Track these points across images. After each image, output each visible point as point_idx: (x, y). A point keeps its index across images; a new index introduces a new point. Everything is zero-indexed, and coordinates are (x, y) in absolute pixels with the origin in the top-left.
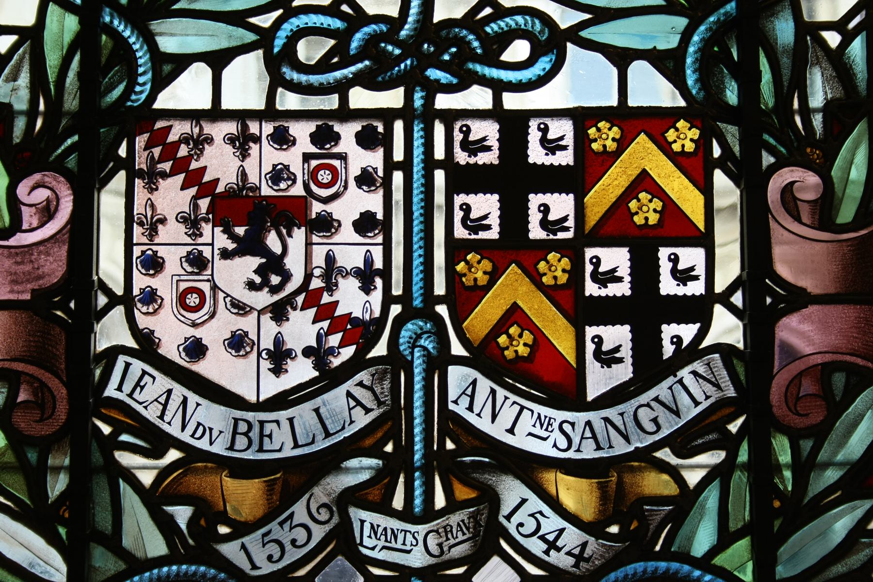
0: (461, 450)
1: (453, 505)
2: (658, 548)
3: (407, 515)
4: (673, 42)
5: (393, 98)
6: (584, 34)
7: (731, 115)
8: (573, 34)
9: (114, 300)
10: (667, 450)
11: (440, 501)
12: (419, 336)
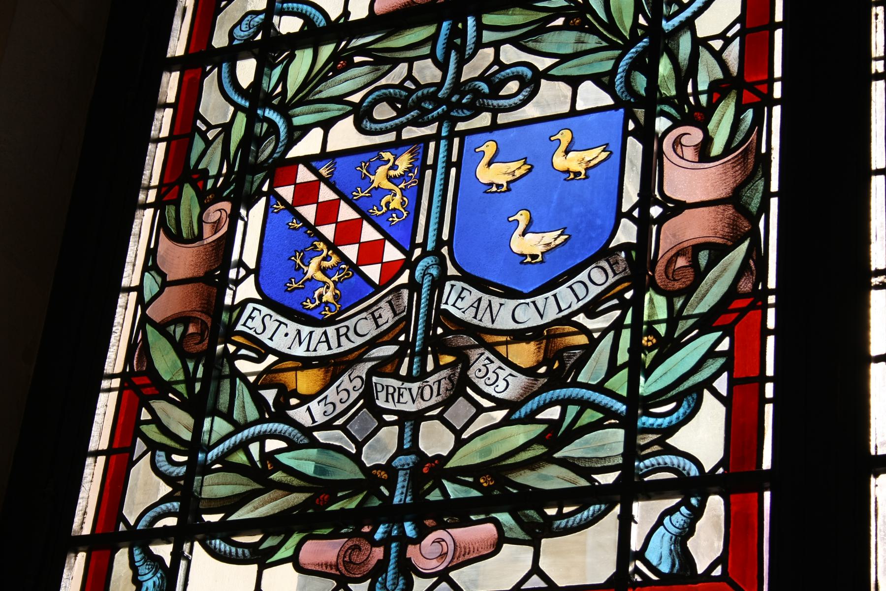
0: (447, 331)
1: (438, 368)
2: (569, 381)
3: (409, 378)
4: (608, 66)
6: (553, 72)
7: (640, 102)
8: (546, 75)
9: (249, 272)
10: (582, 315)
11: (430, 367)
12: (428, 268)
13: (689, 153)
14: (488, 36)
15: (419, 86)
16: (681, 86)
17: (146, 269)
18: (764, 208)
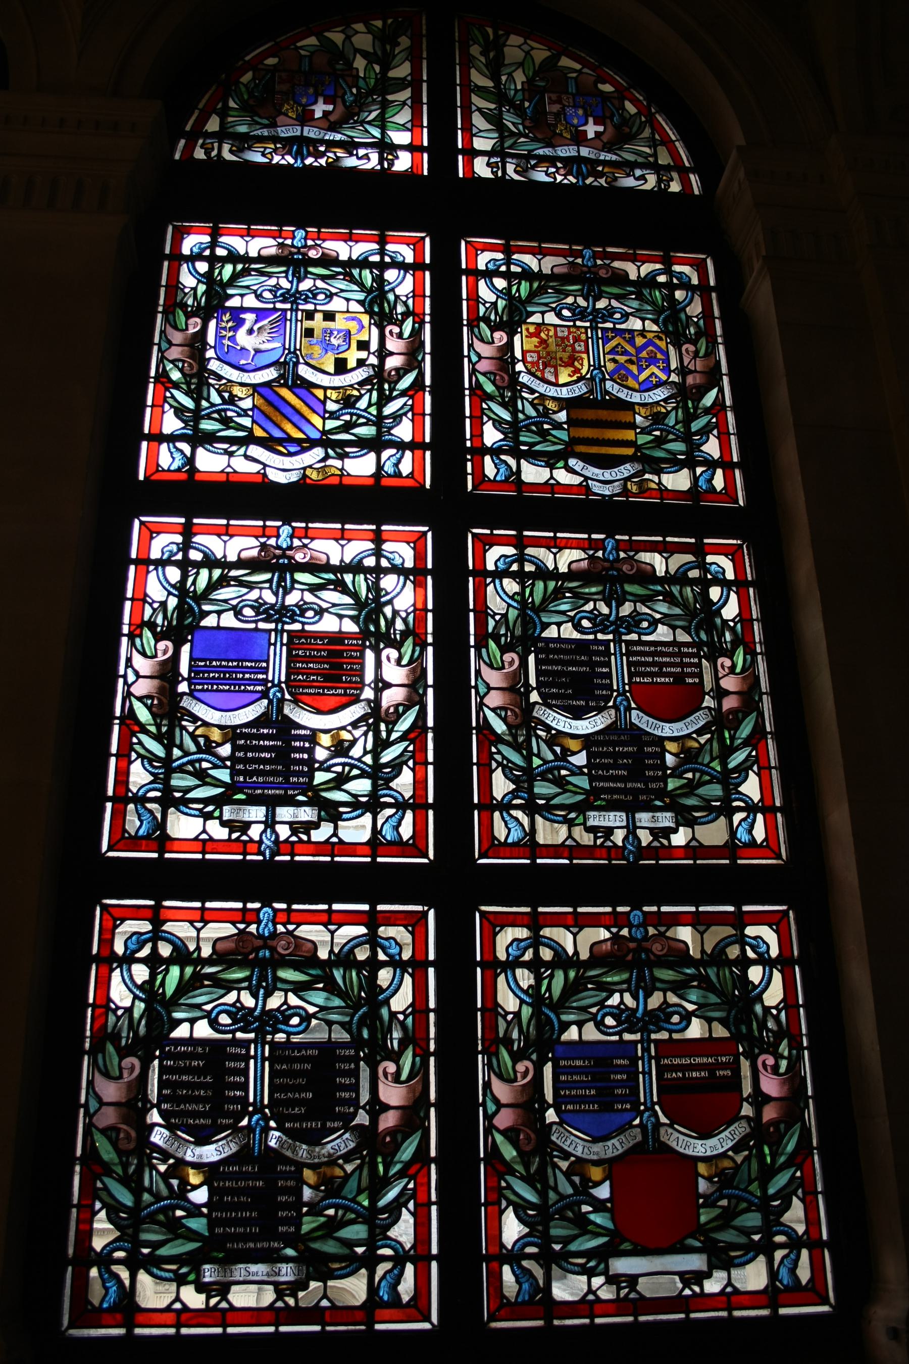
5: (272, 626)
8: (326, 610)
13: (393, 661)
14: (296, 586)
15: (266, 603)
16: (388, 626)
17: (127, 667)
18: (425, 693)
